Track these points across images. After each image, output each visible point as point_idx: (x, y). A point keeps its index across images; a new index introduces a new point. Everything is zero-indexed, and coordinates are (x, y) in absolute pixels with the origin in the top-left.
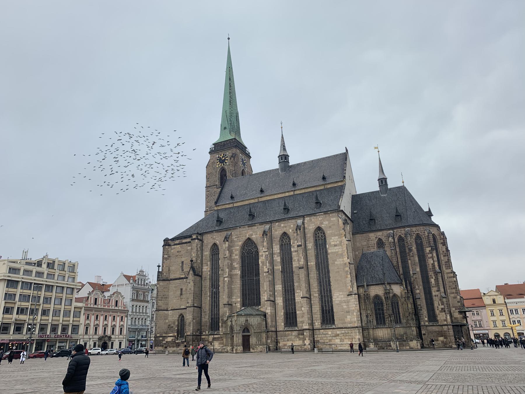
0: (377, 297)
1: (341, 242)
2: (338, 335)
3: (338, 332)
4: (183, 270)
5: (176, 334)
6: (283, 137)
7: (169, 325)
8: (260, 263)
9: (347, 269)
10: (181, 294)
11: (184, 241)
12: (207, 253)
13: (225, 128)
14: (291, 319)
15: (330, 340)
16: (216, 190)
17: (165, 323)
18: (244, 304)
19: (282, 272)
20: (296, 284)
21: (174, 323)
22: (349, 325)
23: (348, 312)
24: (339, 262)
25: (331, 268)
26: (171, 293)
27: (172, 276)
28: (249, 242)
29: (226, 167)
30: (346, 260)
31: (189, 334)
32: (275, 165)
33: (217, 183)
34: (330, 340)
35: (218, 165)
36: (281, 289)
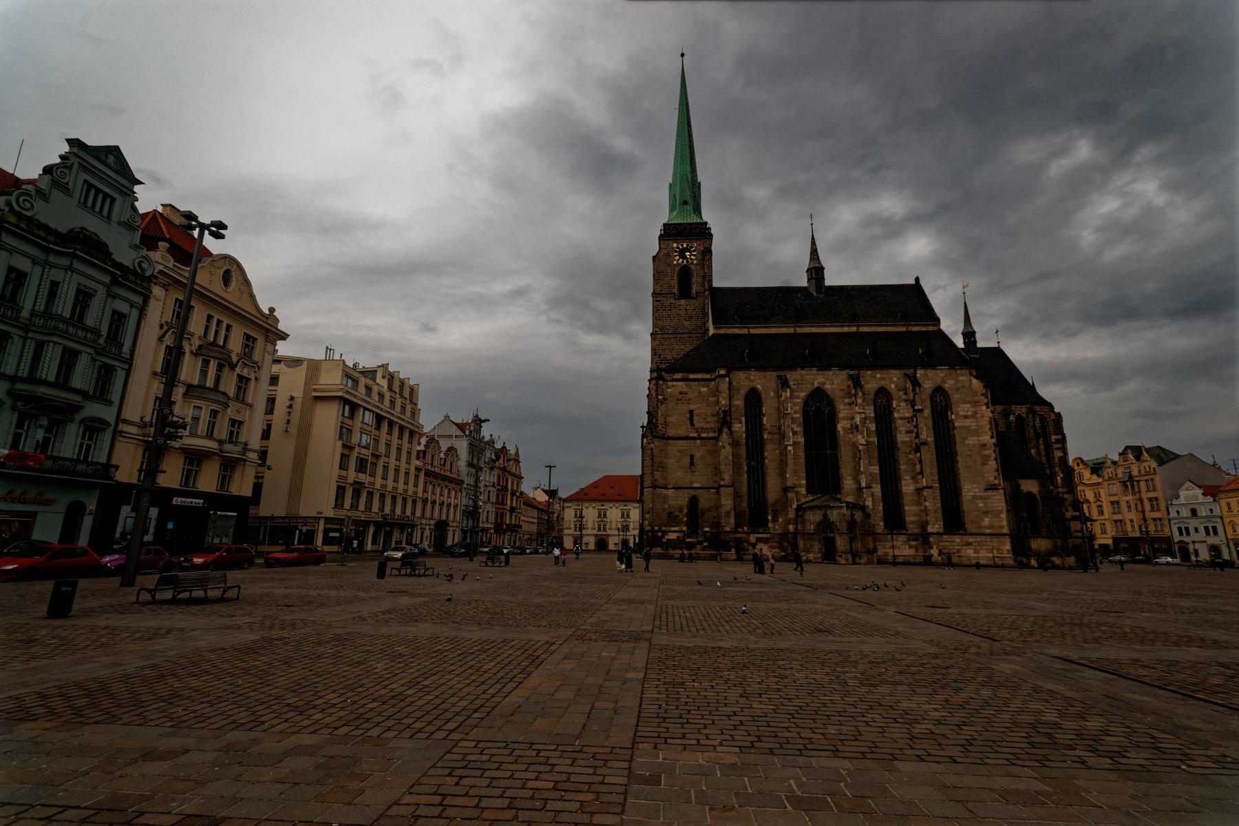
0: (1030, 494)
1: (976, 413)
2: (969, 544)
3: (971, 540)
4: (692, 424)
5: (685, 528)
6: (813, 238)
7: (670, 513)
8: (839, 429)
9: (989, 452)
10: (692, 464)
11: (692, 376)
12: (739, 402)
13: (685, 203)
14: (895, 519)
15: (959, 551)
16: (672, 301)
17: (664, 510)
18: (810, 490)
19: (879, 445)
20: (903, 467)
21: (681, 510)
22: (988, 531)
23: (986, 513)
24: (972, 440)
25: (959, 448)
26: (671, 462)
27: (672, 433)
28: (818, 395)
29: (693, 267)
30: (987, 438)
31: (728, 529)
32: (802, 281)
33: (675, 290)
34: (959, 551)
35: (677, 260)
36: (877, 471)
